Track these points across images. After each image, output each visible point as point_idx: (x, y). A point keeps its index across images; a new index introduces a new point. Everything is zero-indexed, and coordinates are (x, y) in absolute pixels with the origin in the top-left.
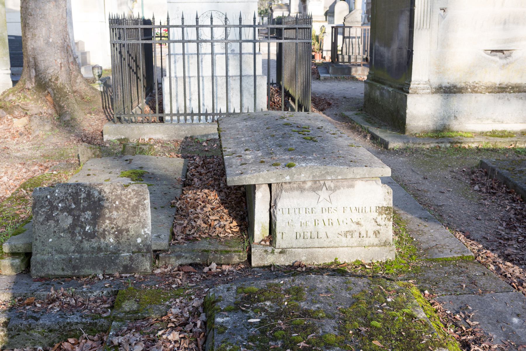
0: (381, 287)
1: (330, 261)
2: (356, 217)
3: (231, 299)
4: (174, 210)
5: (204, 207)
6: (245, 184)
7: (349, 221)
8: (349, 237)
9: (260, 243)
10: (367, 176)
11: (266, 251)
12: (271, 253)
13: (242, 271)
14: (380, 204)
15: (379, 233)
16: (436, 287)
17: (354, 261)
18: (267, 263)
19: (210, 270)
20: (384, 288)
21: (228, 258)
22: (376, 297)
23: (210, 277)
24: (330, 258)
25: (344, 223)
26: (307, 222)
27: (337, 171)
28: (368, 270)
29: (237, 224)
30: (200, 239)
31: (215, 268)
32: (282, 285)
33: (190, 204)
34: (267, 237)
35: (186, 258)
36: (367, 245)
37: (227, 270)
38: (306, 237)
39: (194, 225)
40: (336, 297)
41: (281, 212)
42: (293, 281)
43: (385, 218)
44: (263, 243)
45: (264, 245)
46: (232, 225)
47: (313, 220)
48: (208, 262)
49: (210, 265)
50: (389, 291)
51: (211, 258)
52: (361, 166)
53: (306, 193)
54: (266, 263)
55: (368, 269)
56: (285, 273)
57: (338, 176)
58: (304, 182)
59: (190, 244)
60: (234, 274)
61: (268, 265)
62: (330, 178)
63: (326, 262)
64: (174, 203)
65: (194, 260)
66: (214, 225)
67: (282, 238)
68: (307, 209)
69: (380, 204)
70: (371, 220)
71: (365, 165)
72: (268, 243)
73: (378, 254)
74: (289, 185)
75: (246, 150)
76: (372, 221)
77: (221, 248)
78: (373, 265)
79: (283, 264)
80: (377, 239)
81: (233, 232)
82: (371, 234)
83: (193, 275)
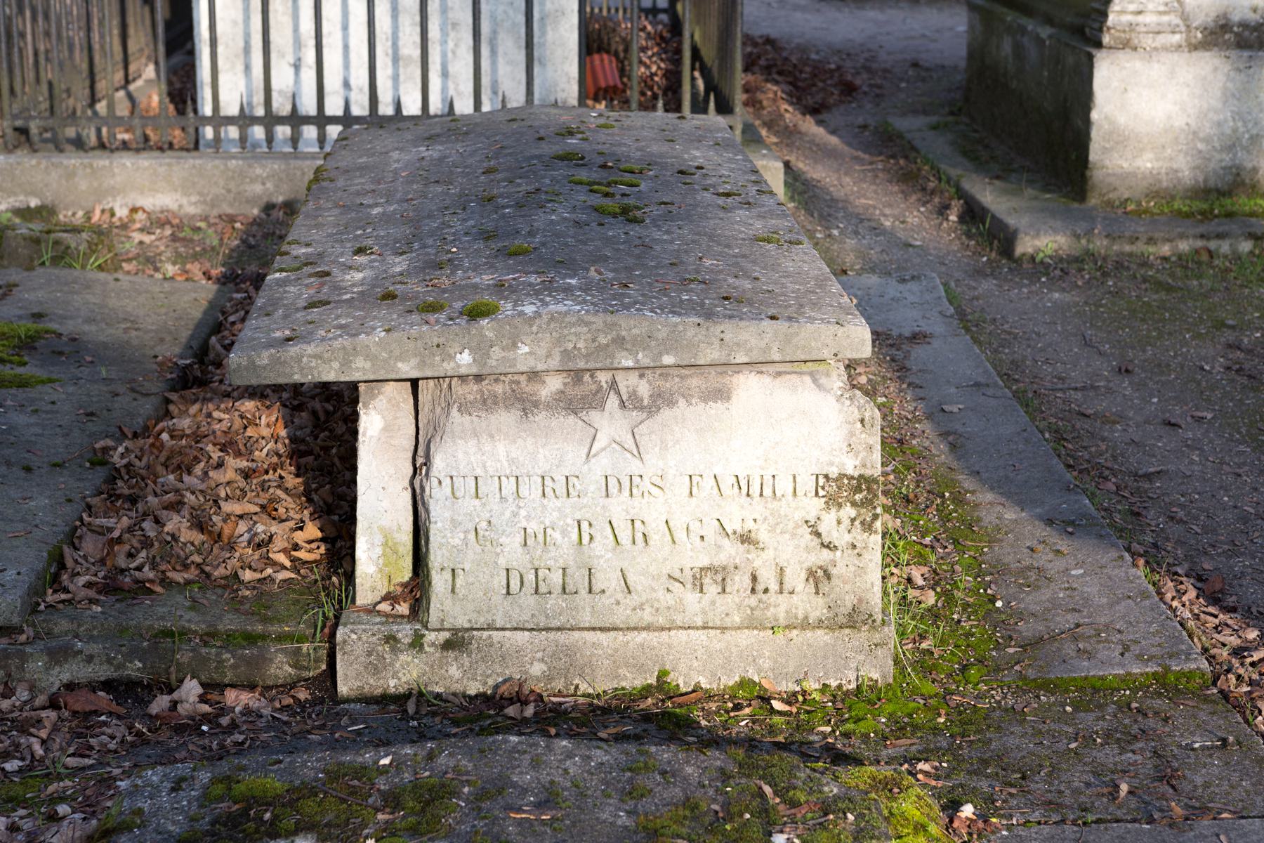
0: (768, 790)
1: (639, 683)
2: (738, 514)
3: (174, 823)
4: (101, 473)
5: (220, 465)
6: (297, 378)
7: (711, 530)
8: (712, 589)
9: (371, 610)
10: (777, 357)
11: (391, 639)
12: (412, 645)
13: (294, 715)
14: (832, 464)
15: (828, 576)
16: (1013, 791)
17: (731, 683)
18: (393, 684)
19: (174, 704)
20: (776, 793)
21: (249, 662)
22: (728, 827)
23: (164, 735)
24: (641, 668)
25: (692, 534)
26: (549, 531)
27: (656, 334)
28: (777, 719)
29: (319, 535)
30: (158, 589)
31: (193, 698)
32: (384, 771)
33: (164, 454)
34: (404, 585)
35: (90, 659)
36: (782, 622)
37: (238, 709)
38: (543, 589)
39: (152, 534)
40: (574, 824)
41: (448, 490)
42: (431, 756)
43: (853, 520)
44: (385, 607)
45: (387, 615)
46: (299, 537)
47: (569, 521)
48: (173, 677)
49: (178, 687)
50: (794, 804)
51: (185, 660)
52: (757, 317)
53: (541, 417)
54: (392, 683)
55: (780, 713)
56: (456, 723)
57: (661, 354)
58: (534, 376)
59: (118, 605)
60: (262, 723)
61: (401, 690)
62: (630, 363)
63: (624, 684)
64: (105, 450)
65: (120, 667)
66: (236, 534)
67: (453, 591)
68: (548, 482)
69: (832, 464)
70: (797, 526)
71: (771, 312)
72: (403, 608)
73: (825, 657)
74: (475, 388)
75: (360, 251)
76: (800, 531)
77: (229, 623)
78: (805, 700)
79: (458, 688)
80: (820, 601)
81: (297, 564)
82: (796, 578)
83: (105, 724)
